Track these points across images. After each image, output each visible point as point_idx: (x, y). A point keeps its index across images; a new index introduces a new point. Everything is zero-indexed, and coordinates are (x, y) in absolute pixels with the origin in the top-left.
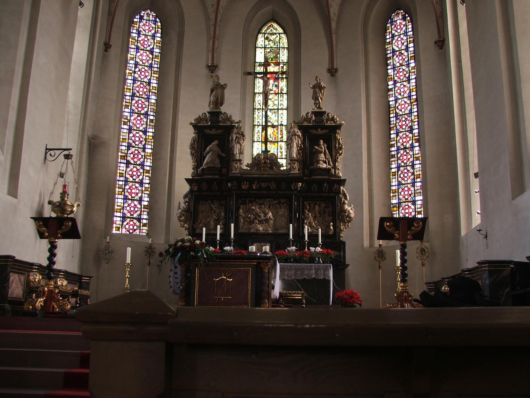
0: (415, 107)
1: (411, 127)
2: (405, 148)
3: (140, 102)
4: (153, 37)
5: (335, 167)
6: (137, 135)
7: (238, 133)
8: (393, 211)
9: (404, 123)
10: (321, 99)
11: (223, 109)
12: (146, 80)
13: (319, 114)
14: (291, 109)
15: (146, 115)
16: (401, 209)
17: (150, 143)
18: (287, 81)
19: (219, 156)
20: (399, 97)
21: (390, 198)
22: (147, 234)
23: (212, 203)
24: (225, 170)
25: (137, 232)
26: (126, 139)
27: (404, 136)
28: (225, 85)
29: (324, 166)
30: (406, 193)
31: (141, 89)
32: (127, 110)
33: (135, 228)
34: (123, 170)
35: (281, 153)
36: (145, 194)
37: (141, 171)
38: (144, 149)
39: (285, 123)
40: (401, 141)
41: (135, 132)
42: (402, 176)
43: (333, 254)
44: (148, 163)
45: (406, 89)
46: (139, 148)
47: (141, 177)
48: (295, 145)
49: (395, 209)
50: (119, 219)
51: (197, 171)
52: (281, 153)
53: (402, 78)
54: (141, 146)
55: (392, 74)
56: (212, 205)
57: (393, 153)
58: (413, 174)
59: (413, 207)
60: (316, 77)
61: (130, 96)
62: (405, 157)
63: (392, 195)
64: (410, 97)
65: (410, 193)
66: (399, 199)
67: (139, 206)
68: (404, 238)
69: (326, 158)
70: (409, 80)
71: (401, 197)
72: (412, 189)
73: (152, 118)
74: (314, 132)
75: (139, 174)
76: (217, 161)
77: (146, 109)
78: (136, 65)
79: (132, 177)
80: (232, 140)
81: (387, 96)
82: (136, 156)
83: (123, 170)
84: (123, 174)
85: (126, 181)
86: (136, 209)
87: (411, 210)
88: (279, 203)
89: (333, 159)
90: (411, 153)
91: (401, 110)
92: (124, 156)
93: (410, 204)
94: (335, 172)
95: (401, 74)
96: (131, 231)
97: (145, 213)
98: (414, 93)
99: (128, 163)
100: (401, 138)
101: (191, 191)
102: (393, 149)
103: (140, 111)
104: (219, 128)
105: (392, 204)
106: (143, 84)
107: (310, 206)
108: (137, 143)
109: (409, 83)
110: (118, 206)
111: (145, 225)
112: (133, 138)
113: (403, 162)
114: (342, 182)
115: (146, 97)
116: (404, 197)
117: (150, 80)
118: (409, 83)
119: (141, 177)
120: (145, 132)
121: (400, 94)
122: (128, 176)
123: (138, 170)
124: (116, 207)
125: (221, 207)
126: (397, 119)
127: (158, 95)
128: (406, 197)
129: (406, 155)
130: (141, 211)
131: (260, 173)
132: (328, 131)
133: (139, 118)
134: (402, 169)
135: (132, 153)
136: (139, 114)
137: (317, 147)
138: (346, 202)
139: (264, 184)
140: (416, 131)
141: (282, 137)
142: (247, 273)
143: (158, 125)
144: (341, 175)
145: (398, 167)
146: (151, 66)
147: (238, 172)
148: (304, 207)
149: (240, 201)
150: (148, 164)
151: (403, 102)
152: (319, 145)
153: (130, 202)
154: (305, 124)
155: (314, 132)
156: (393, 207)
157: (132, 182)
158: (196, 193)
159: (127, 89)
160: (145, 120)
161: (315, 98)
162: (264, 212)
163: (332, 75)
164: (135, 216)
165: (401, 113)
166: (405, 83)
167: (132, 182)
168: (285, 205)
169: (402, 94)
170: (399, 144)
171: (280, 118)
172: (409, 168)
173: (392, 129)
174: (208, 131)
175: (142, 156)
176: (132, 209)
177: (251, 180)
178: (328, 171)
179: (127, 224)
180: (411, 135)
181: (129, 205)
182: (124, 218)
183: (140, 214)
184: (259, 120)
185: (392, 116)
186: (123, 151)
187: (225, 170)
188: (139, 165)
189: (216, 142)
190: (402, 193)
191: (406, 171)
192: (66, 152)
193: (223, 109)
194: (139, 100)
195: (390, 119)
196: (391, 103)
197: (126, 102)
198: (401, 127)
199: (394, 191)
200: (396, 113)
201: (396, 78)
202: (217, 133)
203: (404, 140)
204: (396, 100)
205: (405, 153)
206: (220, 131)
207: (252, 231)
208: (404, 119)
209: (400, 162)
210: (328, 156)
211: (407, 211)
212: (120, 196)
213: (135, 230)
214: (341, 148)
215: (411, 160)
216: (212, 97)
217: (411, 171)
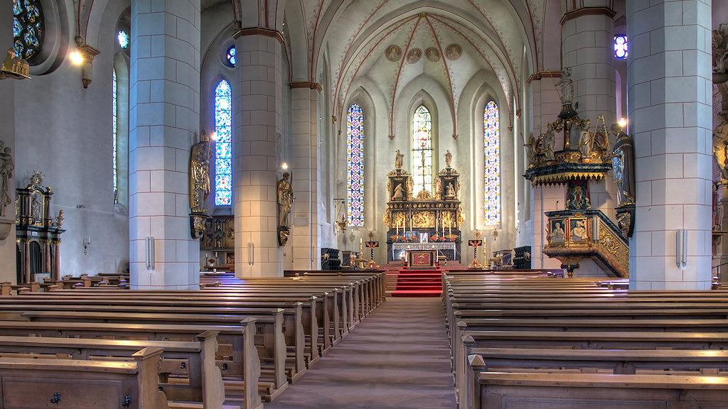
4: (359, 120)
11: (402, 168)
25: (359, 225)
29: (451, 195)
43: (456, 236)
44: (362, 189)
78: (352, 137)
101: (390, 208)
146: (359, 137)
154: (443, 175)
177: (418, 204)
182: (352, 218)
193: (402, 168)
202: (400, 180)
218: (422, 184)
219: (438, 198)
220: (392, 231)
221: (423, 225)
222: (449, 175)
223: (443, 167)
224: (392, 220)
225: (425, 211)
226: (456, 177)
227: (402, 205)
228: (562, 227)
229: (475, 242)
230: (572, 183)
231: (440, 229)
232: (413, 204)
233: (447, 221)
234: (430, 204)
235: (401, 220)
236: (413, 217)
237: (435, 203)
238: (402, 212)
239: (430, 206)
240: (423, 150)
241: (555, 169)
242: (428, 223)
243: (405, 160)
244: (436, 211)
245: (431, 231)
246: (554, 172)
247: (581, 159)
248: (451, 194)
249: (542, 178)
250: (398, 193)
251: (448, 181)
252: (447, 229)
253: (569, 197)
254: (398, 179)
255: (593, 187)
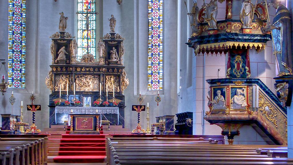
0: (162, 24)
1: (159, 35)
2: (156, 45)
3: (17, 17)
5: (120, 60)
6: (17, 36)
7: (75, 44)
8: (149, 77)
9: (156, 32)
10: (114, 27)
11: (66, 31)
12: (19, 4)
13: (113, 34)
14: (98, 21)
15: (21, 25)
16: (153, 76)
17: (24, 40)
18: (95, 5)
19: (65, 54)
20: (154, 18)
21: (147, 70)
22: (25, 88)
23: (62, 76)
24: (68, 61)
25: (20, 87)
26: (11, 38)
27: (156, 39)
28: (67, 17)
29: (115, 60)
30: (155, 68)
31: (17, 10)
32: (11, 22)
33: (19, 85)
34: (11, 55)
35: (93, 44)
36: (23, 67)
37: (21, 55)
38: (21, 43)
39: (94, 28)
40: (154, 41)
41: (16, 34)
42: (154, 59)
43: (120, 101)
45: (157, 14)
46: (18, 43)
47: (20, 58)
48: (102, 50)
49: (150, 76)
50: (10, 81)
51: (55, 61)
52: (93, 44)
53: (156, 7)
54: (19, 42)
55: (151, 5)
56: (62, 77)
57: (150, 47)
58: (159, 59)
59: (158, 75)
60: (112, 15)
61: (12, 14)
62: (155, 50)
63: (148, 69)
64: (159, 19)
65: (157, 68)
66: (152, 71)
67: (20, 74)
68: (139, 111)
69: (116, 56)
70: (159, 10)
71: (153, 70)
72: (158, 66)
73: (24, 26)
74: (110, 43)
75: (19, 57)
76: (65, 57)
77: (21, 21)
79: (16, 58)
80: (71, 46)
81: (148, 17)
82: (17, 47)
83: (11, 55)
84: (11, 57)
85: (13, 61)
86: (19, 75)
87: (157, 77)
88: (94, 77)
89: (120, 56)
90: (158, 48)
91: (154, 25)
92: (11, 48)
93: (157, 74)
94: (120, 62)
95: (156, 5)
96: (17, 87)
97: (24, 77)
98: (161, 17)
99: (13, 51)
100: (154, 40)
101: (53, 71)
102: (150, 45)
103: (18, 22)
104: (64, 40)
105: (148, 73)
106: (18, 7)
107: (108, 78)
108: (17, 40)
109: (159, 11)
110: (10, 74)
111: (23, 83)
112: (15, 38)
113: (154, 52)
114: (123, 68)
115: (20, 14)
116: (154, 70)
117: (21, 5)
118: (159, 11)
119: (20, 58)
120: (21, 34)
121: (154, 16)
122: (13, 58)
123: (19, 55)
124: (9, 75)
125: (66, 78)
126: (152, 29)
127: (26, 13)
128: (155, 70)
129: (156, 49)
130: (21, 76)
131: (85, 63)
132: (117, 42)
133: (17, 26)
134: (154, 56)
135: (15, 46)
136: (17, 24)
137: (112, 51)
138: (125, 77)
139: (87, 69)
140: (161, 38)
141: (93, 36)
142: (92, 119)
143: (28, 29)
144: (123, 64)
145: (152, 55)
147: (75, 63)
148: (106, 79)
149: (76, 76)
150: (24, 51)
151: (156, 21)
152: (112, 50)
153: (15, 71)
154: (107, 39)
155: (110, 43)
156: (149, 75)
157: (16, 61)
158: (55, 72)
159: (10, 10)
160: (21, 27)
161: (111, 26)
162: (88, 82)
163: (119, 4)
164: (18, 79)
165: (154, 27)
166: (157, 11)
167: (16, 61)
168: (97, 78)
169: (155, 16)
170: (153, 43)
171: (92, 26)
172: (157, 56)
173: (150, 34)
174: (59, 41)
175: (20, 47)
176: (17, 75)
177: (81, 67)
178: (117, 62)
179: (15, 83)
180: (158, 39)
181: (15, 73)
182: (13, 80)
183: (21, 78)
184: (81, 27)
185: (150, 27)
186: (10, 45)
187: (68, 61)
188: (19, 52)
189: (64, 47)
190: (154, 68)
191: (156, 57)
192: (3, 61)
193: (66, 31)
194: (16, 16)
195: (149, 29)
196: (150, 21)
197: (10, 18)
198: (154, 34)
199: (150, 67)
200: (152, 27)
201: (153, 7)
203: (156, 41)
204: (152, 20)
205: (156, 48)
206: (65, 42)
207: (82, 90)
208: (156, 30)
209: (153, 52)
210: (117, 55)
211: (155, 77)
212: (10, 69)
213: (19, 86)
214: (123, 51)
215: (158, 52)
216: (60, 24)
217: (158, 58)
218: (85, 47)
219: (102, 63)
220: (55, 94)
221: (87, 89)
222: (113, 40)
223: (107, 31)
224: (54, 82)
225: (88, 74)
226: (120, 42)
227: (65, 68)
228: (223, 94)
229: (139, 107)
230: (233, 52)
231: (104, 93)
232: (76, 67)
233: (111, 86)
234: (94, 68)
235: (64, 83)
236: (77, 81)
237: (99, 68)
238: (66, 75)
239: (94, 70)
240: (87, 13)
241: (217, 38)
242: (91, 86)
243: (69, 23)
244: (99, 75)
245: (95, 95)
246: (216, 41)
247: (242, 29)
248: (114, 58)
249: (205, 46)
250: (61, 56)
251: (112, 45)
252: (110, 94)
253: (230, 65)
254: (62, 42)
255: (252, 57)
